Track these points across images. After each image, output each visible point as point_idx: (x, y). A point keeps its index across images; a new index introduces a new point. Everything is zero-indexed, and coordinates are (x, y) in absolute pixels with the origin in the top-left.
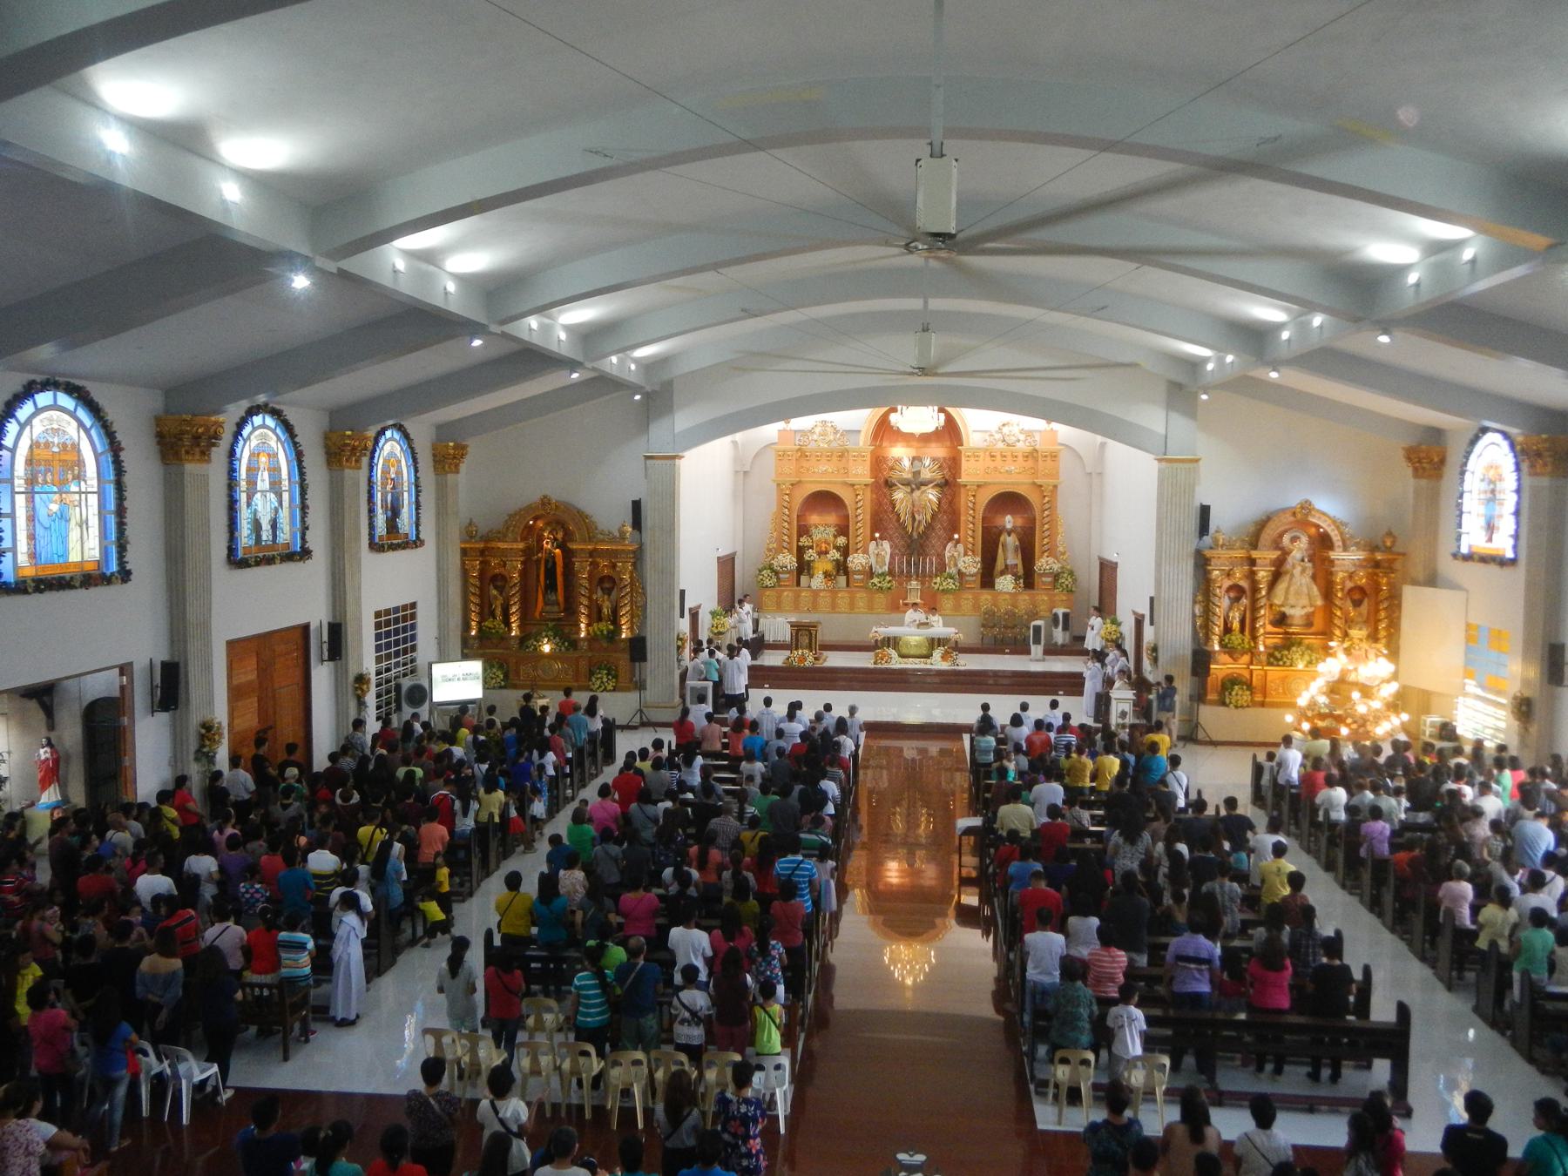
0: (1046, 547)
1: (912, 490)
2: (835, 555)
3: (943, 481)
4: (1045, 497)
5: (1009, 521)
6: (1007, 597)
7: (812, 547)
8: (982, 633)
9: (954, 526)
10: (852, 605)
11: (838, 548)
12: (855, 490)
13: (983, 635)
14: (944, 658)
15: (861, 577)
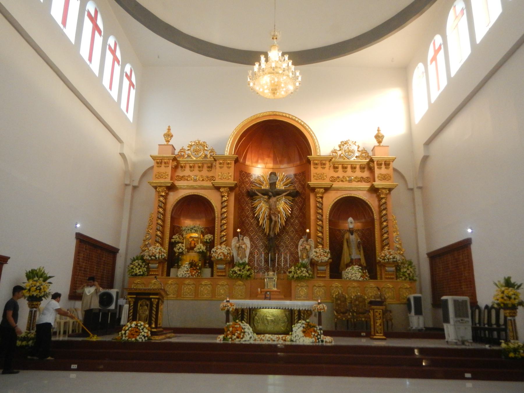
0: (385, 243)
1: (270, 197)
2: (201, 247)
3: (295, 191)
4: (382, 198)
5: (351, 223)
6: (355, 284)
7: (182, 243)
8: (336, 317)
9: (304, 223)
10: (213, 293)
11: (205, 243)
12: (221, 192)
13: (338, 319)
14: (306, 332)
15: (223, 266)
